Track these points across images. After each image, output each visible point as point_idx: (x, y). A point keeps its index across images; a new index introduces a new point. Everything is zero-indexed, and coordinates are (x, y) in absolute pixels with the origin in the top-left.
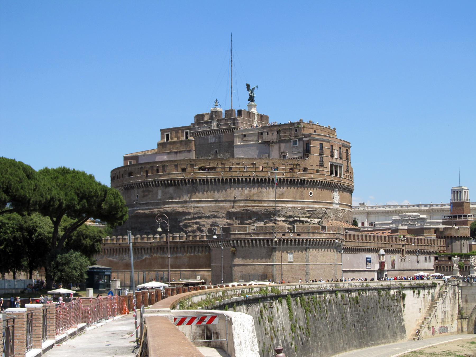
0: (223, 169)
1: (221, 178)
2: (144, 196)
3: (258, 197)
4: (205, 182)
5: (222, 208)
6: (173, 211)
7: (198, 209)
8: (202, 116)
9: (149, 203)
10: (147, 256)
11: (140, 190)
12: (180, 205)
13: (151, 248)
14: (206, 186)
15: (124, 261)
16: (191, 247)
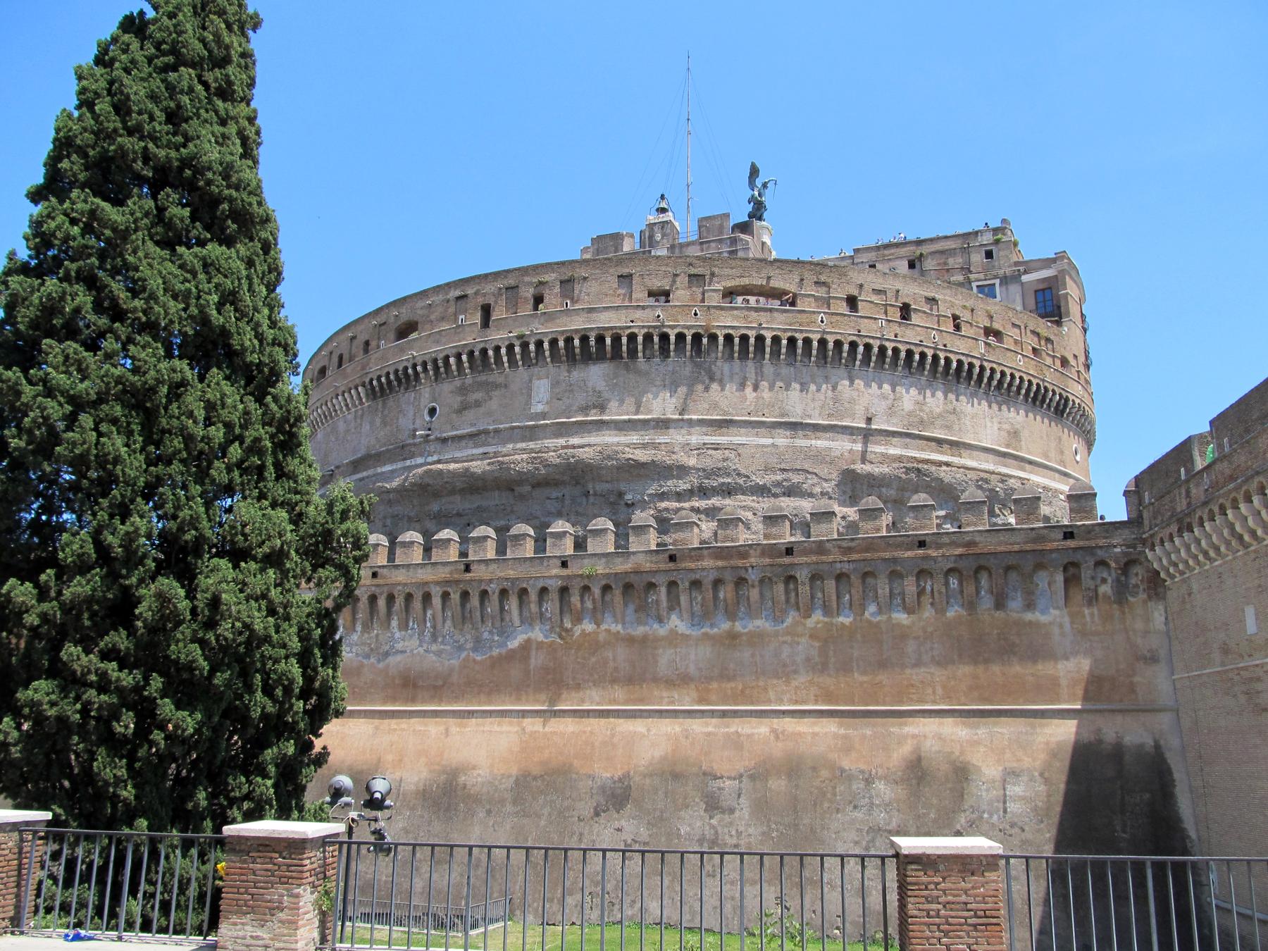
0: (827, 302)
1: (815, 337)
2: (464, 408)
3: (947, 427)
4: (746, 348)
5: (820, 457)
6: (609, 458)
7: (718, 454)
8: (617, 238)
9: (486, 432)
10: (537, 634)
11: (446, 387)
12: (634, 438)
13: (564, 591)
14: (750, 363)
15: (392, 660)
16: (840, 577)
